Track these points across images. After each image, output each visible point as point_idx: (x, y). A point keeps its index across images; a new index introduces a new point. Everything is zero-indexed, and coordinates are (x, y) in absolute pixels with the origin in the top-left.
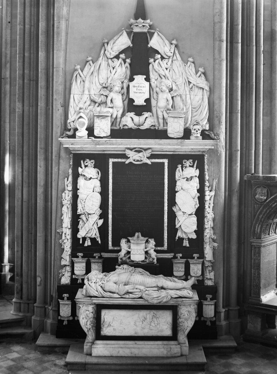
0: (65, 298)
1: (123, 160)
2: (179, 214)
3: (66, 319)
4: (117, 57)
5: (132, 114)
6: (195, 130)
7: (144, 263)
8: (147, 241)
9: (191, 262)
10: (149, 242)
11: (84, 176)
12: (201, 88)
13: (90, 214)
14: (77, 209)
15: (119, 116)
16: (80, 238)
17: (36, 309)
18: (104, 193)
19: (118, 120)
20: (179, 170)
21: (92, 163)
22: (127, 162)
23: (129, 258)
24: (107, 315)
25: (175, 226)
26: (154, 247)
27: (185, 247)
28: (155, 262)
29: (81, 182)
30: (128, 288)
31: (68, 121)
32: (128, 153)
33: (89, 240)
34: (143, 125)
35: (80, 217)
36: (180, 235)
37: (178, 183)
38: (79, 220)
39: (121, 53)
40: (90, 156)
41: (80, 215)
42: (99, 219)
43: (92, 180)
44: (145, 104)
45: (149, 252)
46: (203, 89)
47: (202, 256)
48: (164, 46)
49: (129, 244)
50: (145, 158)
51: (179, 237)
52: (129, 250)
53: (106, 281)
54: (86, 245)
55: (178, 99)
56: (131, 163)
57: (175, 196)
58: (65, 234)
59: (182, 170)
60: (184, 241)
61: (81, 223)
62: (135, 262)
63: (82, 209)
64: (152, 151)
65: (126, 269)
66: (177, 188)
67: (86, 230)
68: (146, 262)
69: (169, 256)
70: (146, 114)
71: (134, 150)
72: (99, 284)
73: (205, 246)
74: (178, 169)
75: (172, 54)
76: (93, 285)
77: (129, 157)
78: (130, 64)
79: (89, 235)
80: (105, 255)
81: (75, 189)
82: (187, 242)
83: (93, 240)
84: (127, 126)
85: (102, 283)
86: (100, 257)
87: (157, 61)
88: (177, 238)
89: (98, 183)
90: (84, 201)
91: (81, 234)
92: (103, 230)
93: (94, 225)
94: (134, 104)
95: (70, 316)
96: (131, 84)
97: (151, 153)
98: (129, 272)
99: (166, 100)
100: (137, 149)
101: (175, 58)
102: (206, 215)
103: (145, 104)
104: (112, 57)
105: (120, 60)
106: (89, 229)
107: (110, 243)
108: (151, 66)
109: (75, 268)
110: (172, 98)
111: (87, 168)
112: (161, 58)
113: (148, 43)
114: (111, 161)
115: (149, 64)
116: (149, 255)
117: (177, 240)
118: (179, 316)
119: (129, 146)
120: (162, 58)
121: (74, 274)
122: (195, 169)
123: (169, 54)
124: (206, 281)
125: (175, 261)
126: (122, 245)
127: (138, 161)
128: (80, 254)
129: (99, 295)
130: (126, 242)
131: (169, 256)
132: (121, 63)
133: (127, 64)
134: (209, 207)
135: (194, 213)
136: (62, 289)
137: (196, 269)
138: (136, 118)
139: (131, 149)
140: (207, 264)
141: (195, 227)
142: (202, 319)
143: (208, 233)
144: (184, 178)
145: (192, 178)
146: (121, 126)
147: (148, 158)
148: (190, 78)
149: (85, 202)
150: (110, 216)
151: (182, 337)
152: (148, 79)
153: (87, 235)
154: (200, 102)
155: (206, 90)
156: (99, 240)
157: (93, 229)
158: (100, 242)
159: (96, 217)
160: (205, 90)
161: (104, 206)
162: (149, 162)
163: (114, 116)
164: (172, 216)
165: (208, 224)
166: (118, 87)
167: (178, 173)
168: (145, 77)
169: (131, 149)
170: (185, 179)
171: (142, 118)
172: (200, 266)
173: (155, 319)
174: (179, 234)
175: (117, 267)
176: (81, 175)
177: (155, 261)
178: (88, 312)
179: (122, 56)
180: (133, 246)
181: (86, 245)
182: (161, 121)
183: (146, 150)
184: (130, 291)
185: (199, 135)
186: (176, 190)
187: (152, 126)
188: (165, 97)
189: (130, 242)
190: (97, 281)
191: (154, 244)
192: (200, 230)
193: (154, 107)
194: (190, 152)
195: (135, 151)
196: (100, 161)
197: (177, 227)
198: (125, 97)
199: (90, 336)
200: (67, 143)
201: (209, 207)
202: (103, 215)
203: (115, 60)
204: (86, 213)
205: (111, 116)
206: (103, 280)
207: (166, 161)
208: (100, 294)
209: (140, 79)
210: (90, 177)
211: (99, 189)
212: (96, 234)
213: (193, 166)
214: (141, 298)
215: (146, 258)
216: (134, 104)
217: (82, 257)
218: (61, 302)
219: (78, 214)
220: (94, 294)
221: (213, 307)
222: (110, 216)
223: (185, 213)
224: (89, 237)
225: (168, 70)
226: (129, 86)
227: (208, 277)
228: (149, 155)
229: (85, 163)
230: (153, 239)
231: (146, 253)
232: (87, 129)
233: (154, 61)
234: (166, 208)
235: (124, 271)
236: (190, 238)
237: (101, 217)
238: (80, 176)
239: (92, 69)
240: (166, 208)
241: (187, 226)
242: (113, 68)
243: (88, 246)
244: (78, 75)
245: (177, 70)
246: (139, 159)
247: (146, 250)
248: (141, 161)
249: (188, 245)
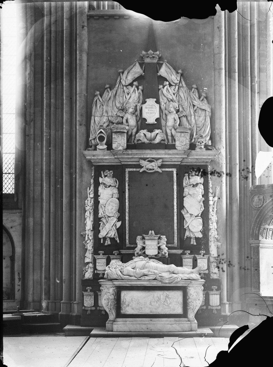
0: (89, 290)
1: (138, 170)
2: (186, 216)
3: (89, 309)
4: (131, 84)
5: (145, 131)
6: (199, 142)
7: (157, 257)
8: (160, 238)
9: (197, 258)
10: (161, 238)
11: (104, 184)
12: (204, 109)
13: (109, 217)
14: (98, 213)
15: (134, 134)
16: (101, 238)
17: (62, 305)
18: (121, 198)
19: (133, 137)
20: (186, 178)
21: (111, 173)
22: (141, 170)
23: (144, 253)
24: (126, 296)
25: (184, 226)
26: (165, 243)
27: (193, 245)
29: (101, 189)
30: (145, 271)
31: (90, 139)
32: (143, 163)
33: (109, 240)
34: (154, 140)
35: (101, 220)
36: (188, 234)
37: (186, 190)
38: (100, 223)
39: (134, 81)
40: (109, 168)
41: (101, 218)
42: (118, 221)
43: (111, 187)
44: (156, 123)
45: (162, 247)
46: (206, 110)
47: (208, 252)
48: (171, 75)
49: (144, 240)
50: (157, 167)
51: (187, 237)
54: (106, 244)
55: (184, 119)
56: (144, 172)
57: (183, 200)
58: (88, 235)
59: (189, 178)
60: (192, 240)
61: (101, 225)
63: (102, 213)
64: (163, 162)
65: (142, 259)
66: (185, 194)
67: (106, 231)
68: (159, 256)
69: (179, 252)
70: (157, 131)
71: (147, 160)
73: (210, 245)
74: (185, 177)
75: (179, 82)
77: (143, 167)
78: (142, 91)
79: (109, 235)
80: (123, 251)
81: (96, 196)
82: (194, 240)
83: (112, 239)
84: (141, 141)
86: (119, 254)
87: (166, 87)
88: (185, 237)
89: (116, 191)
90: (104, 206)
91: (102, 234)
92: (121, 231)
93: (114, 227)
94: (146, 123)
95: (93, 307)
96: (144, 106)
97: (161, 163)
99: (174, 120)
100: (149, 159)
101: (181, 85)
102: (210, 217)
103: (156, 123)
104: (127, 84)
105: (134, 87)
106: (109, 230)
107: (127, 241)
108: (160, 92)
109: (97, 264)
110: (179, 118)
111: (106, 177)
112: (169, 84)
113: (158, 72)
114: (127, 170)
115: (159, 90)
117: (186, 239)
118: (188, 296)
119: (142, 157)
120: (170, 85)
121: (97, 270)
122: (200, 177)
123: (176, 82)
124: (212, 275)
125: (184, 256)
126: (137, 241)
127: (151, 169)
128: (101, 252)
130: (142, 239)
131: (179, 252)
132: (134, 89)
133: (140, 91)
134: (213, 211)
135: (200, 215)
136: (85, 283)
137: (202, 263)
138: (149, 135)
139: (144, 159)
140: (212, 259)
141: (201, 227)
142: (209, 307)
143: (213, 233)
144: (190, 185)
145: (197, 184)
146: (135, 142)
147: (159, 167)
148: (194, 102)
149: (105, 206)
150: (127, 218)
151: (191, 315)
152: (158, 102)
153: (108, 235)
154: (203, 122)
155: (208, 111)
156: (118, 239)
157: (112, 230)
158: (118, 241)
159: (115, 219)
160: (207, 111)
161: (121, 210)
162: (159, 170)
163: (130, 133)
164: (181, 218)
165: (213, 226)
166: (133, 108)
167: (185, 182)
168: (155, 100)
169: (144, 159)
170: (192, 186)
171: (153, 134)
172: (206, 261)
173: (168, 299)
174: (187, 234)
176: (102, 184)
177: (167, 255)
178: (109, 294)
179: (135, 83)
180: (147, 242)
181: (106, 244)
182: (170, 138)
183: (157, 159)
184: (146, 273)
185: (203, 147)
186: (184, 195)
187: (162, 140)
188: (173, 117)
189: (145, 239)
190: (117, 267)
192: (206, 230)
193: (164, 126)
194: (195, 162)
195: (148, 161)
196: (118, 171)
197: (185, 227)
198: (138, 119)
199: (112, 316)
200: (89, 154)
201: (213, 211)
202: (121, 218)
203: (130, 87)
204: (106, 216)
205: (127, 133)
207: (175, 171)
208: (120, 277)
209: (151, 102)
210: (109, 185)
211: (116, 196)
212: (115, 235)
213: (198, 175)
214: (155, 279)
215: (159, 253)
216: (146, 123)
217: (103, 254)
218: (85, 293)
219: (99, 217)
221: (218, 296)
222: (127, 218)
223: (192, 215)
224: (109, 237)
225: (176, 95)
226: (142, 108)
227: (214, 271)
228: (160, 164)
229: (105, 173)
230: (164, 236)
231: (159, 248)
232: (106, 144)
233: (163, 87)
234: (175, 210)
235: (140, 260)
236: (197, 237)
237: (119, 219)
238: (101, 184)
239: (110, 94)
240: (175, 210)
241: (194, 227)
242: (128, 94)
243: (109, 245)
244: (98, 100)
245: (183, 95)
246: (151, 168)
247: (158, 245)
248: (153, 169)
249: (195, 244)
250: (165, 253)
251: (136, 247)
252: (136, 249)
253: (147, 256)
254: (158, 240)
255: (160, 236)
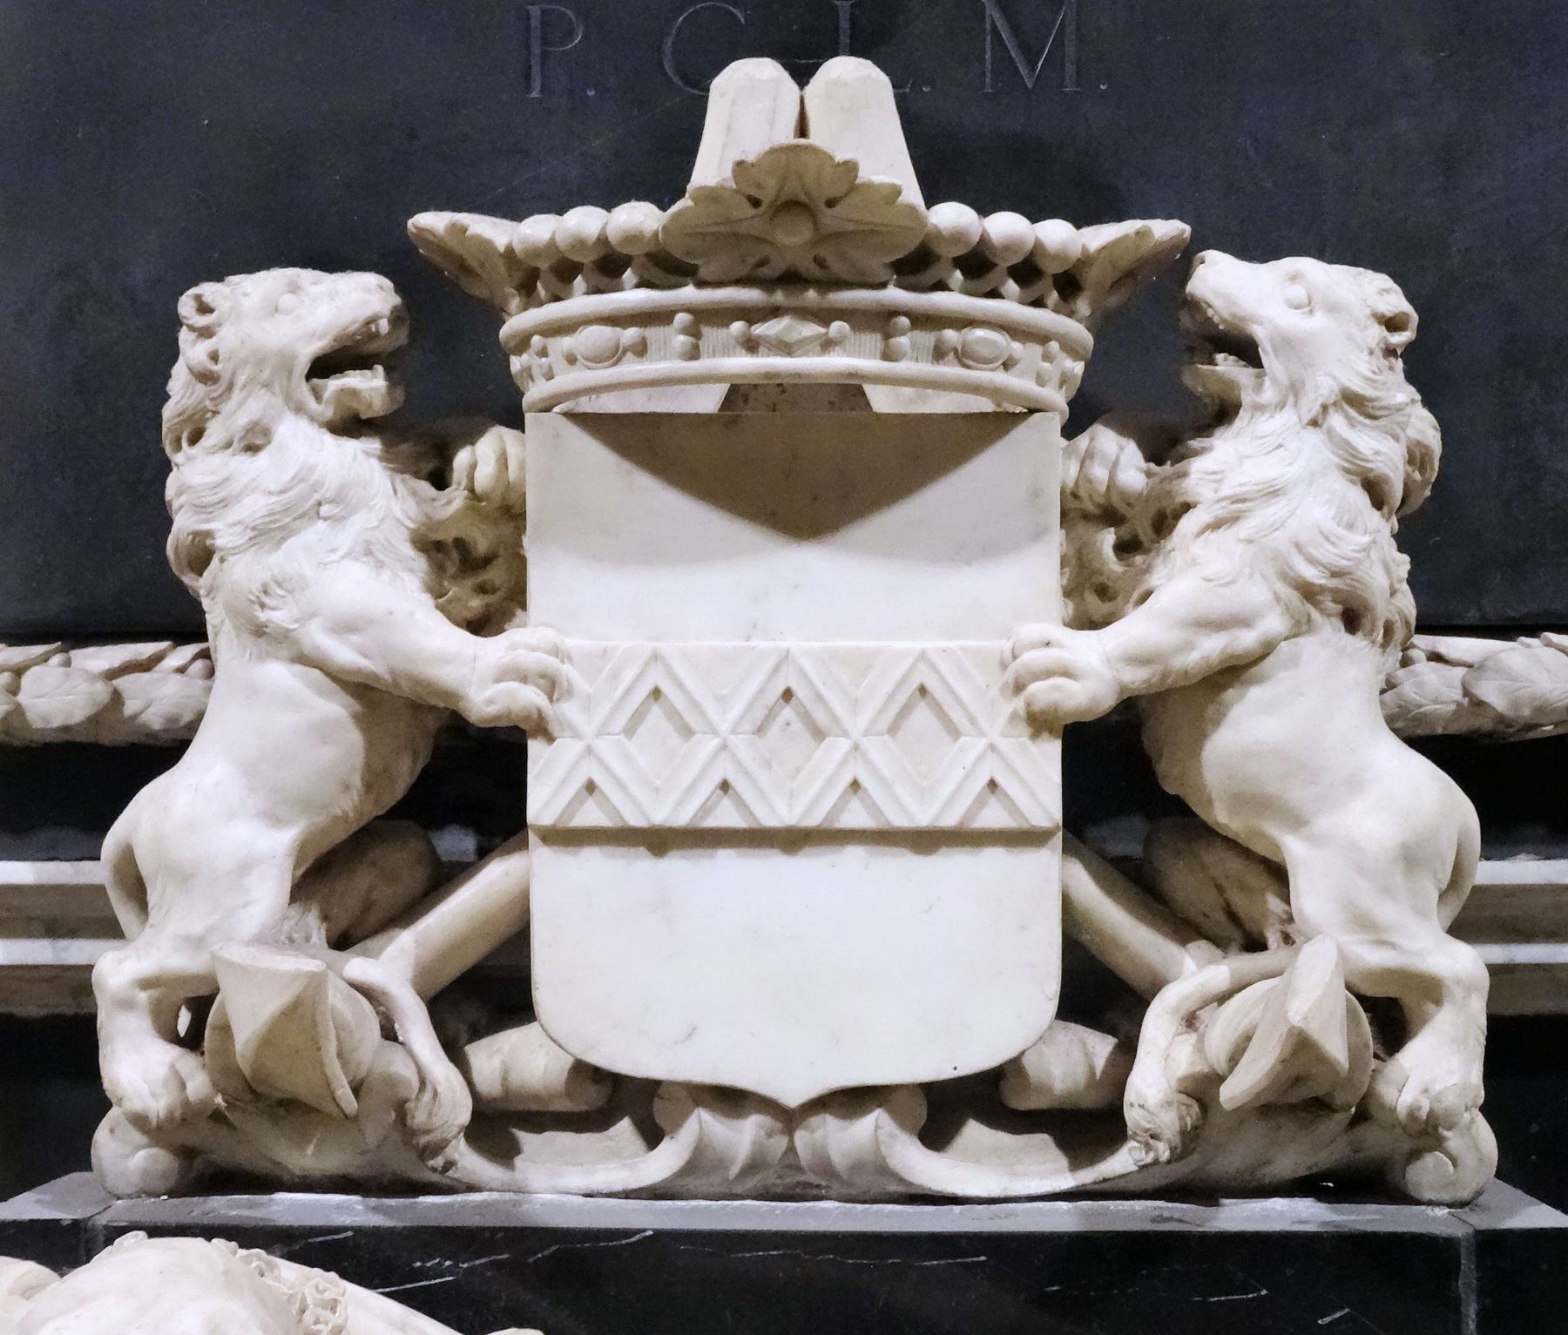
23: (488, 991)
28: (1427, 1133)
45: (1239, 748)
52: (481, 675)
62: (702, 1123)
116: (1185, 881)
130: (370, 385)
177: (1441, 1068)
191: (1386, 454)
215: (1099, 993)
231: (1126, 783)
247: (1095, 668)
250: (1389, 1016)
251: (160, 752)
252: (152, 817)
253: (612, 1099)
254: (1071, 430)
255: (1181, 261)
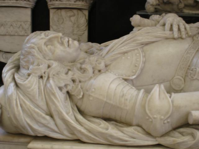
53: (90, 70)
65: (175, 28)
72: (62, 85)
76: (32, 83)
85: (74, 81)
98: (189, 40)
129: (62, 134)
175: (136, 19)
206: (79, 66)
220: (36, 127)
235: (168, 33)
